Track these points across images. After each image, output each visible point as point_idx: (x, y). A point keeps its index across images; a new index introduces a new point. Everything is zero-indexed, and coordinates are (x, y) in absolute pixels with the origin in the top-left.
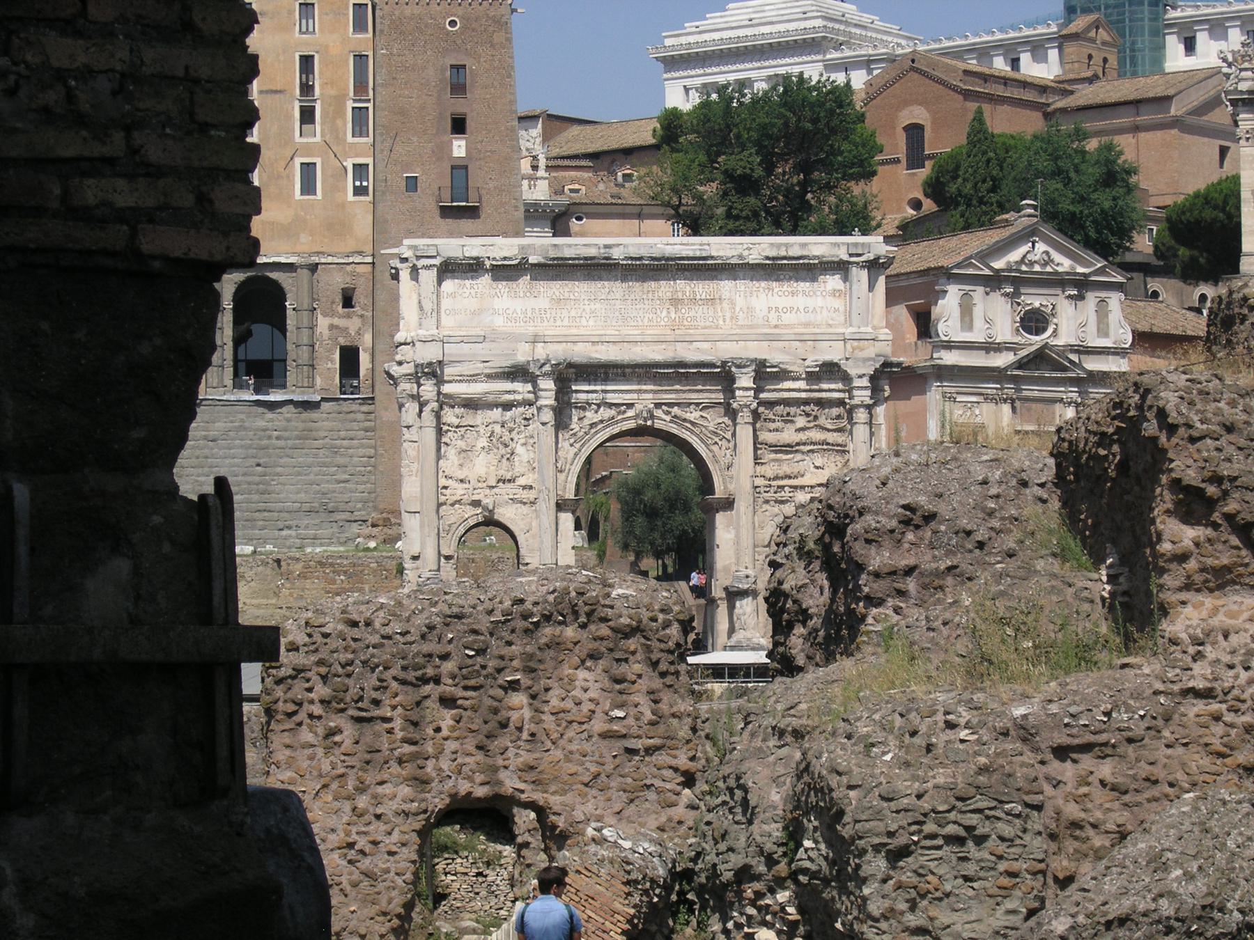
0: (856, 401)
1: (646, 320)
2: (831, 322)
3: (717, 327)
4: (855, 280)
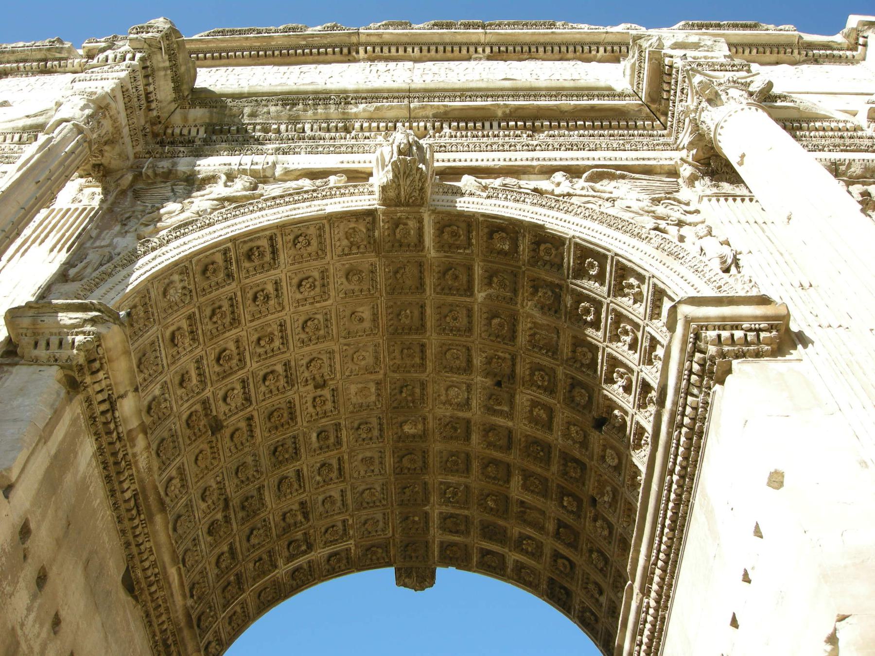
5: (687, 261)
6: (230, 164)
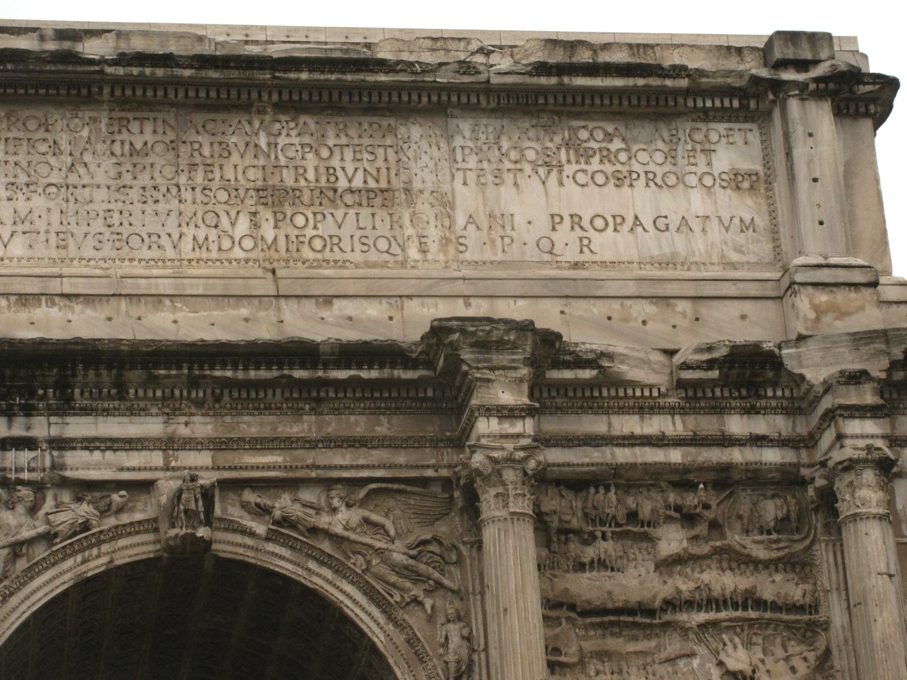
0: (848, 452)
1: (187, 245)
2: (735, 257)
3: (403, 264)
4: (798, 132)
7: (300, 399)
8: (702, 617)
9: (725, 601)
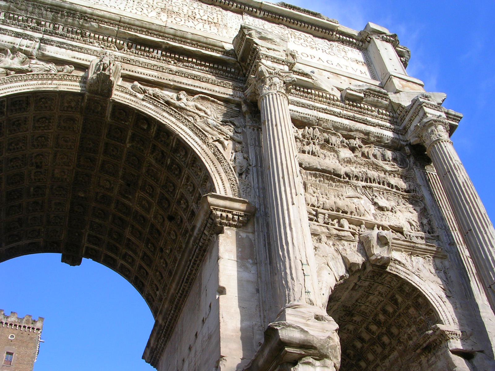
5: (224, 165)
6: (14, 44)
7: (171, 57)
8: (364, 184)
9: (374, 180)
